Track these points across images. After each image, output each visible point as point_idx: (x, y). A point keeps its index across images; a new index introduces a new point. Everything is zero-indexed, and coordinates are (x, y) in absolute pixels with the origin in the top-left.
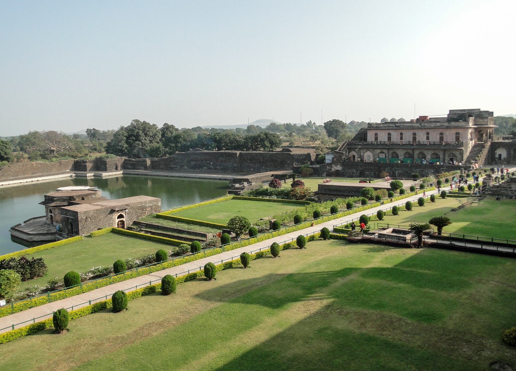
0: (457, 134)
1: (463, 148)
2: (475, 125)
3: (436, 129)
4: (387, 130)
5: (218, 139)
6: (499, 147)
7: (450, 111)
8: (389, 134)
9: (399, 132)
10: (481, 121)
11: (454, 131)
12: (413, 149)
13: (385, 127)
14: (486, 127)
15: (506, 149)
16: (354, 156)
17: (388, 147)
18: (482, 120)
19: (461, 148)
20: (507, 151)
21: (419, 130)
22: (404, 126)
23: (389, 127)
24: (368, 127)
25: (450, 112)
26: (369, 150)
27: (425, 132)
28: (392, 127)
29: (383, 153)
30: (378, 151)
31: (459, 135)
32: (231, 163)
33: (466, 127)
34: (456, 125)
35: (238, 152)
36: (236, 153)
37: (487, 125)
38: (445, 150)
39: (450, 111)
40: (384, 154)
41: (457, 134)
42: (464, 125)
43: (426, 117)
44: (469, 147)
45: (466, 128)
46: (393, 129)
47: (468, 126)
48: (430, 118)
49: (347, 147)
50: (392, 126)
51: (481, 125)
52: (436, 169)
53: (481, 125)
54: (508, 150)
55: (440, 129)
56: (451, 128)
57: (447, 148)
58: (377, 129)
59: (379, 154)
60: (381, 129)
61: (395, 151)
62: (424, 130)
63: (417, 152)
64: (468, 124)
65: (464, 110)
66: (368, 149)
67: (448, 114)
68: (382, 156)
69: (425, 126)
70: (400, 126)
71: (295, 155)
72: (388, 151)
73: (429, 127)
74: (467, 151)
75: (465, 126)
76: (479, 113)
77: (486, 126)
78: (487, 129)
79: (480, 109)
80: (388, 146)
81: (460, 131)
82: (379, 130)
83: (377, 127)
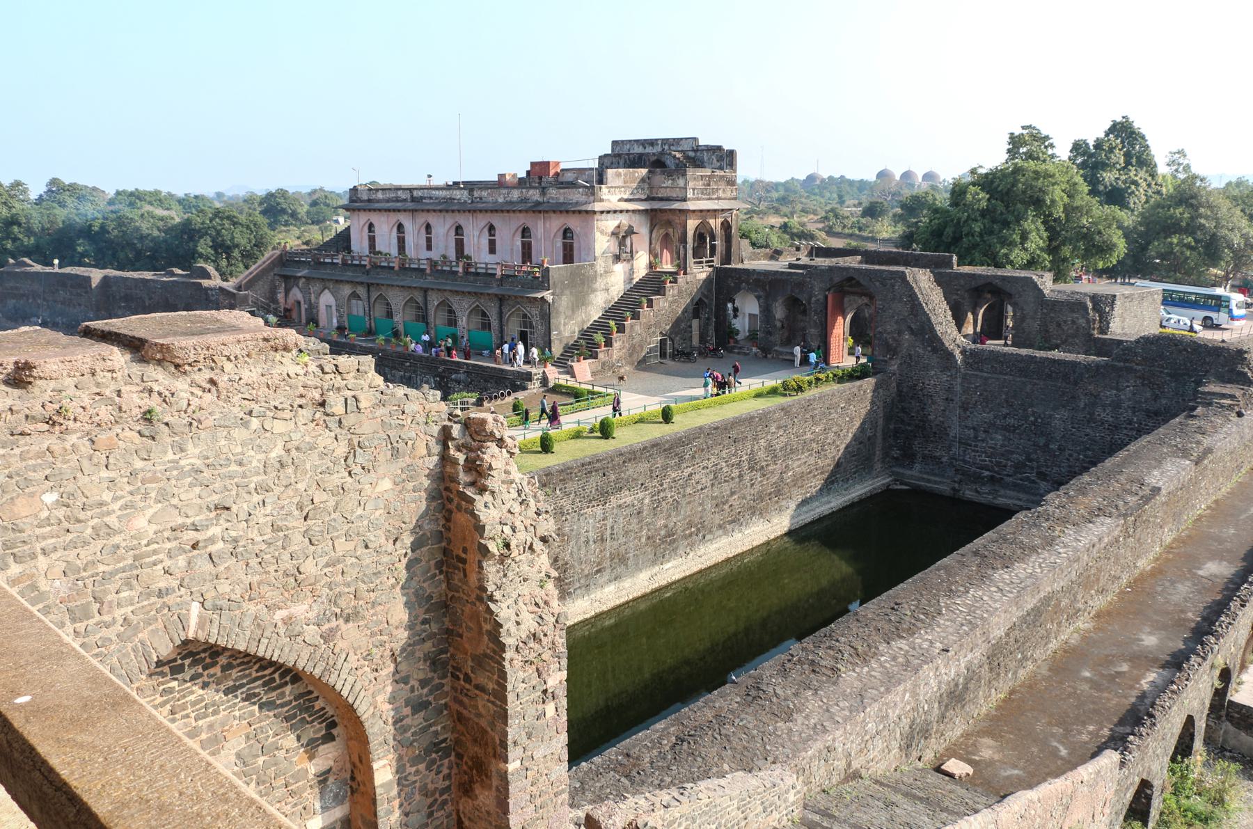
0: (567, 233)
1: (548, 295)
2: (649, 199)
3: (512, 215)
4: (392, 214)
5: (96, 229)
6: (737, 289)
7: (615, 143)
8: (400, 227)
9: (422, 219)
10: (665, 185)
11: (556, 223)
12: (425, 291)
13: (388, 201)
14: (680, 211)
15: (758, 298)
16: (299, 303)
17: (364, 278)
18: (670, 182)
19: (539, 295)
20: (760, 306)
21: (467, 214)
22: (431, 198)
23: (397, 200)
24: (351, 201)
25: (613, 150)
26: (327, 284)
27: (483, 221)
28: (405, 200)
29: (359, 297)
30: (347, 290)
31: (572, 238)
32: (82, 307)
33: (583, 208)
34: (562, 200)
35: (96, 275)
36: (89, 278)
37: (685, 200)
38: (501, 300)
39: (615, 143)
40: (360, 302)
41: (567, 233)
42: (583, 199)
43: (546, 165)
44: (600, 284)
45: (587, 212)
46: (405, 211)
47: (598, 207)
48: (562, 170)
49: (276, 270)
50: (404, 197)
51: (668, 199)
52: (442, 378)
53: (668, 199)
54: (761, 300)
55: (521, 215)
56: (547, 212)
57: (506, 290)
58: (370, 210)
59: (349, 299)
60: (380, 210)
61: (383, 291)
62: (480, 216)
63: (434, 300)
64: (592, 198)
65: (652, 143)
66: (325, 283)
67: (600, 158)
68: (358, 308)
69: (481, 199)
70: (422, 198)
71: (211, 289)
72: (369, 291)
73: (490, 206)
74: (580, 301)
75: (586, 203)
76: (692, 154)
77: (676, 205)
78: (683, 218)
79: (695, 139)
80: (368, 272)
81: (573, 223)
82: (375, 210)
83: (369, 201)
